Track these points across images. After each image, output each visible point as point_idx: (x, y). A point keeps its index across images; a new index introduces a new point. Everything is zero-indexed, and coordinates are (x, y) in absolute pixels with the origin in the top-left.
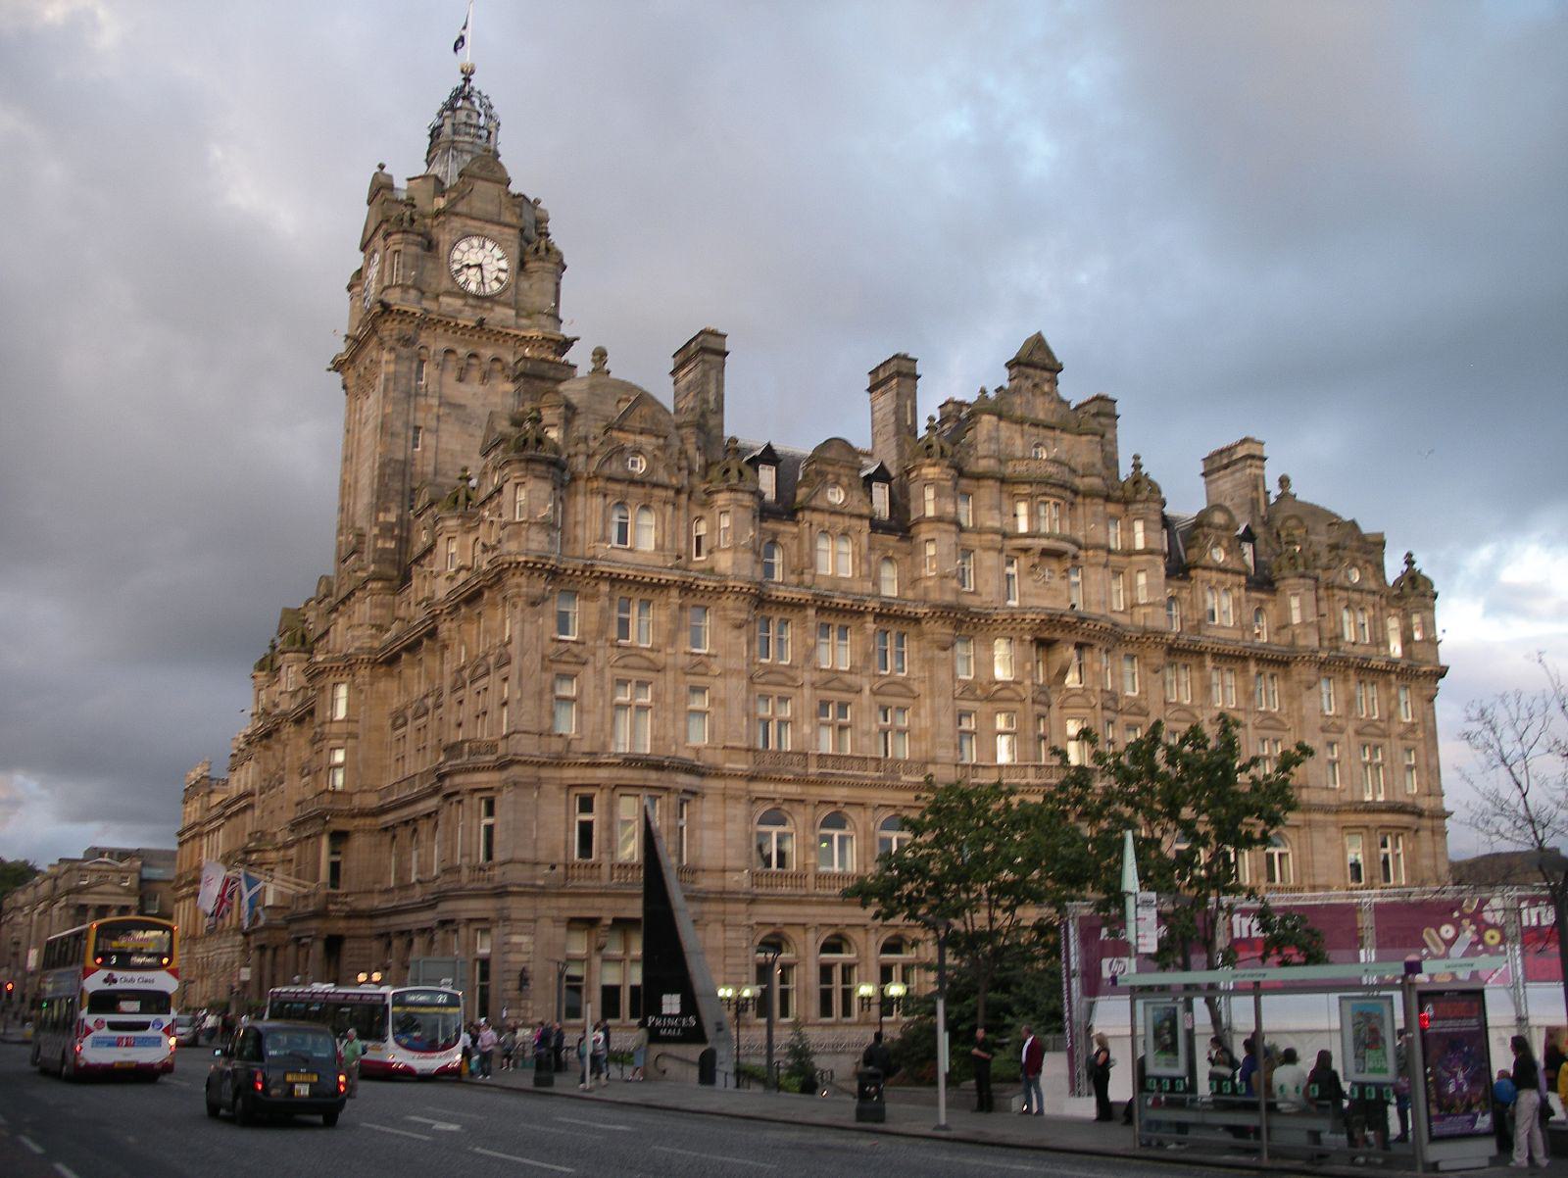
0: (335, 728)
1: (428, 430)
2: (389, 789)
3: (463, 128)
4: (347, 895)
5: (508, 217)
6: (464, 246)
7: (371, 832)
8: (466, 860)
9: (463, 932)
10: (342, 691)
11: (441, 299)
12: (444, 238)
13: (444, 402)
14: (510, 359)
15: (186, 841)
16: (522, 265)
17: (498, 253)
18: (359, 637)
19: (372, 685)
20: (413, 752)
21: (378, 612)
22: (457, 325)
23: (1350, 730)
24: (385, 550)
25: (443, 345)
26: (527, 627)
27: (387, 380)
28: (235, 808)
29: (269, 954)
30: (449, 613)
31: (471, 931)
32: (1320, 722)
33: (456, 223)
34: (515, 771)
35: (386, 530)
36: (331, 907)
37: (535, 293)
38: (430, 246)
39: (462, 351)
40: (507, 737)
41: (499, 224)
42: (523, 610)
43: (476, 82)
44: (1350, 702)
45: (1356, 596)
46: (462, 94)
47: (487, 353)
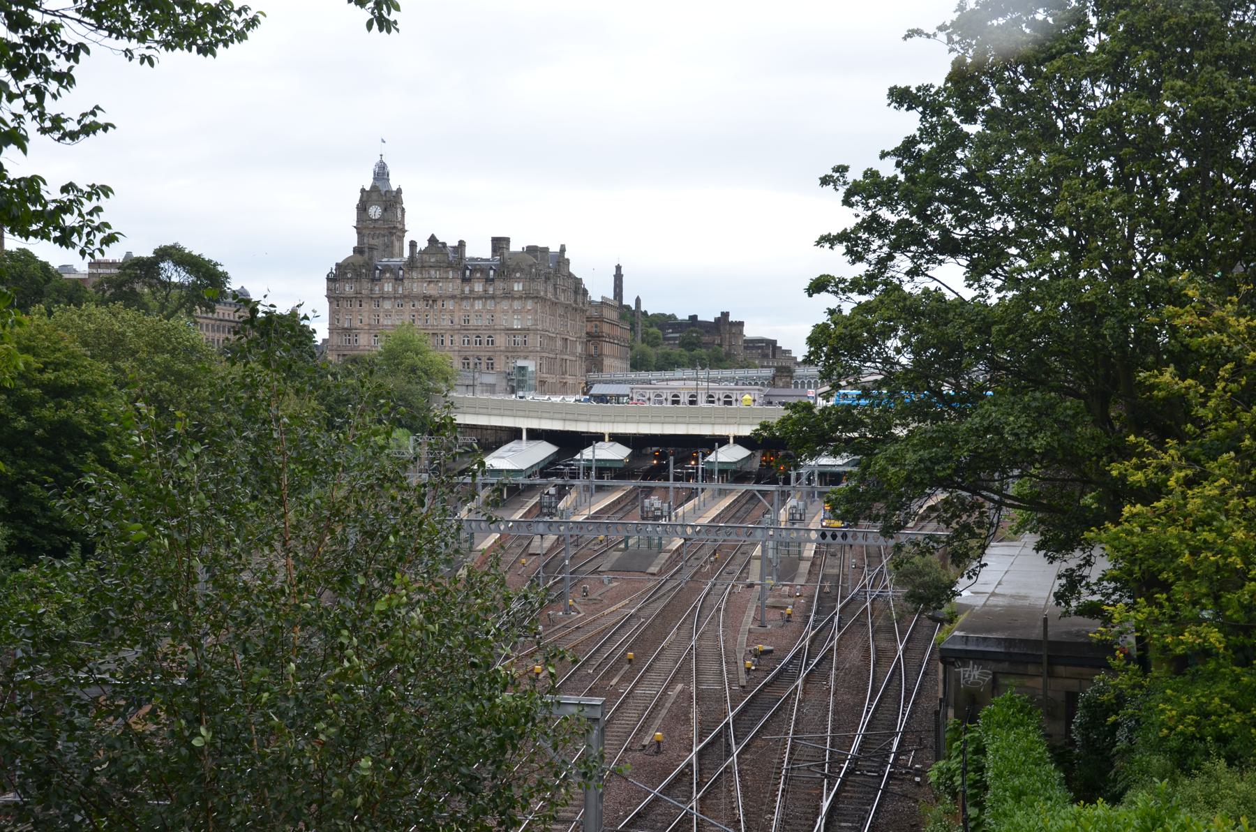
3: (381, 173)
16: (385, 210)
37: (389, 215)
46: (381, 162)
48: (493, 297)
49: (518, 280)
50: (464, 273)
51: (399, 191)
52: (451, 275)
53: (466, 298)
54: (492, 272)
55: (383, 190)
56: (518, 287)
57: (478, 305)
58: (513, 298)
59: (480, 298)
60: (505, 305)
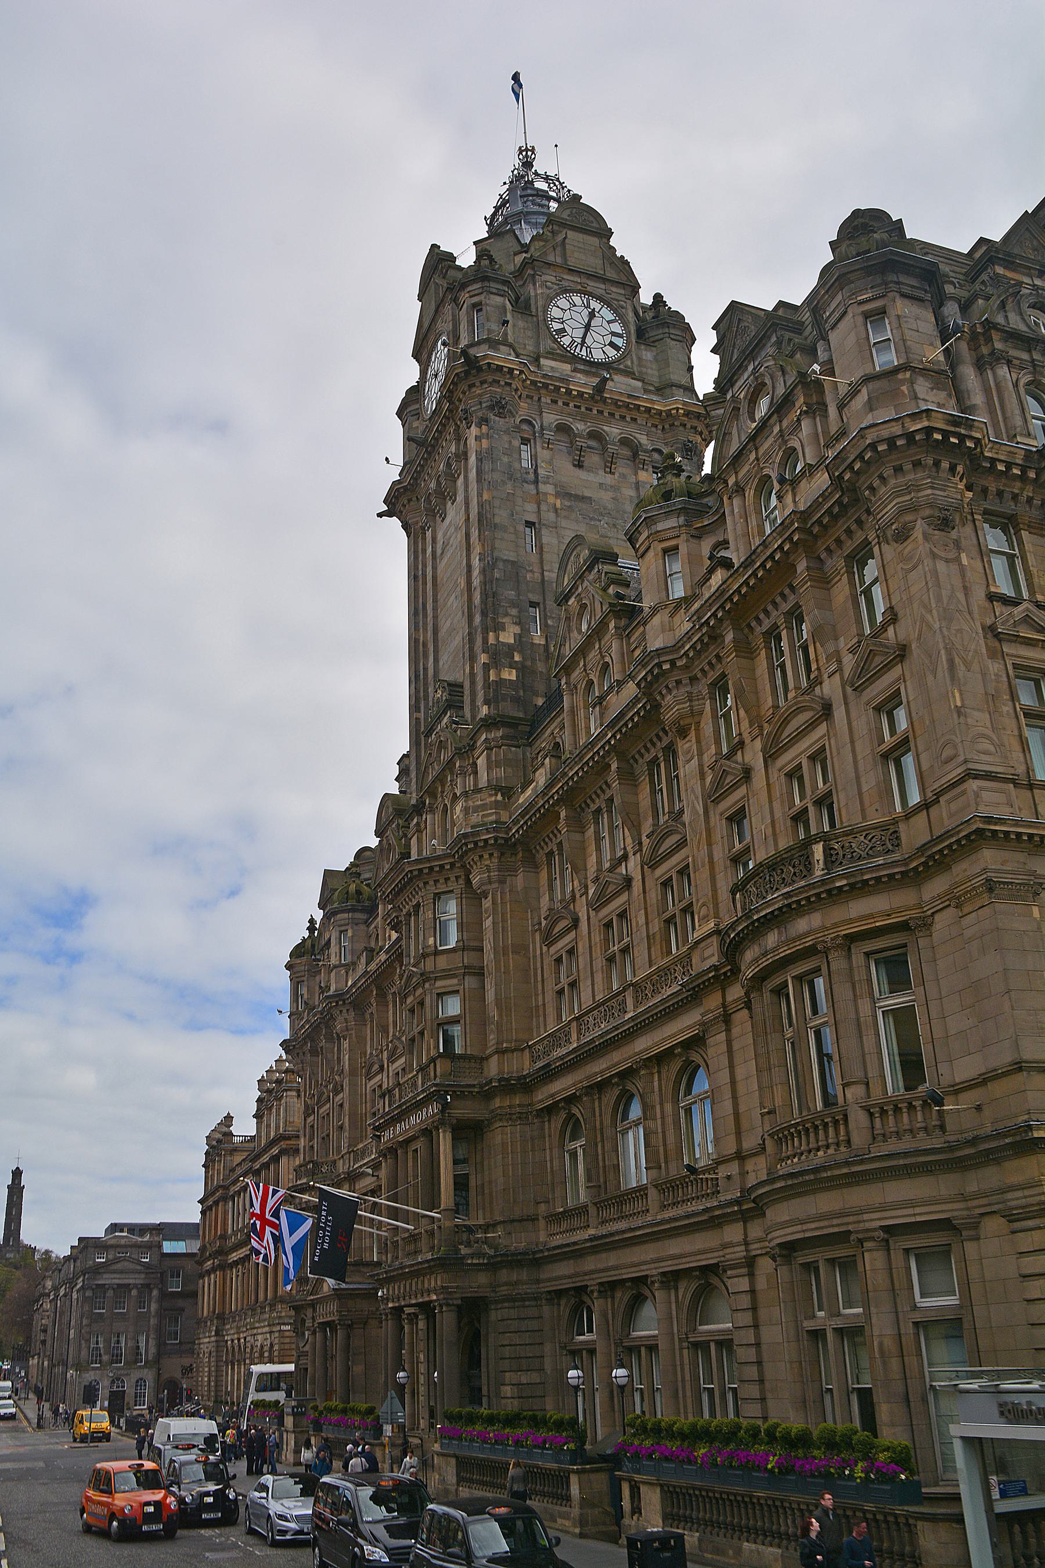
0: (442, 962)
1: (547, 526)
2: (556, 1039)
4: (487, 1227)
6: (563, 303)
7: (522, 1117)
8: (855, 1093)
9: (872, 1261)
10: (452, 907)
11: (543, 361)
12: (535, 291)
13: (563, 493)
15: (210, 1208)
18: (476, 809)
19: (502, 882)
20: (599, 963)
21: (500, 773)
22: (569, 392)
24: (500, 682)
25: (550, 418)
26: (941, 566)
27: (480, 460)
28: (265, 1158)
29: (340, 1334)
30: (686, 667)
31: (897, 1257)
33: (549, 277)
34: (989, 859)
35: (499, 656)
36: (464, 1250)
38: (522, 306)
40: (926, 806)
41: (604, 280)
42: (926, 537)
43: (539, 166)
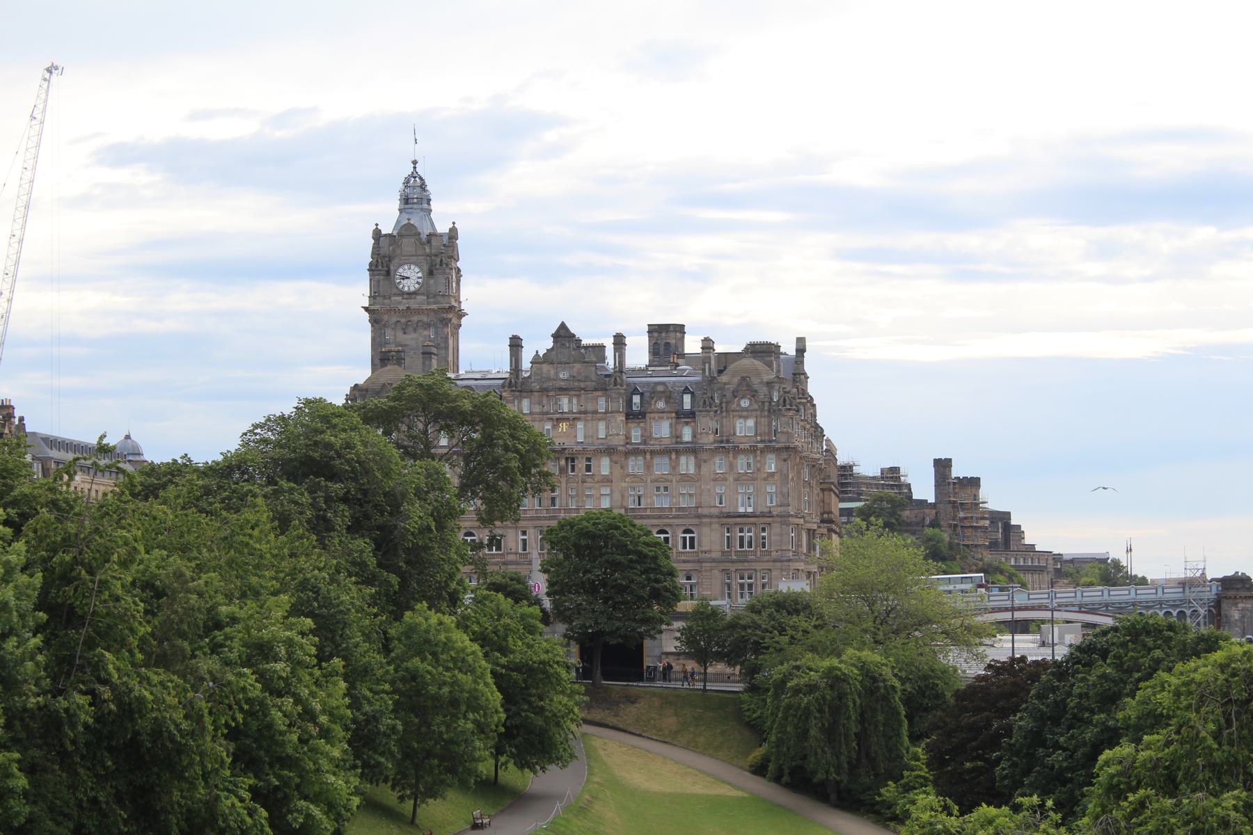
3: (415, 196)
5: (420, 252)
6: (401, 270)
14: (425, 319)
16: (431, 273)
17: (417, 270)
23: (731, 479)
25: (394, 319)
32: (713, 476)
37: (437, 284)
38: (388, 273)
39: (403, 320)
44: (732, 467)
45: (745, 413)
46: (414, 175)
47: (415, 319)
48: (693, 450)
49: (744, 414)
50: (629, 402)
51: (453, 234)
52: (602, 405)
53: (636, 452)
54: (687, 399)
55: (425, 231)
56: (744, 428)
57: (661, 466)
58: (737, 451)
59: (666, 452)
60: (718, 465)
